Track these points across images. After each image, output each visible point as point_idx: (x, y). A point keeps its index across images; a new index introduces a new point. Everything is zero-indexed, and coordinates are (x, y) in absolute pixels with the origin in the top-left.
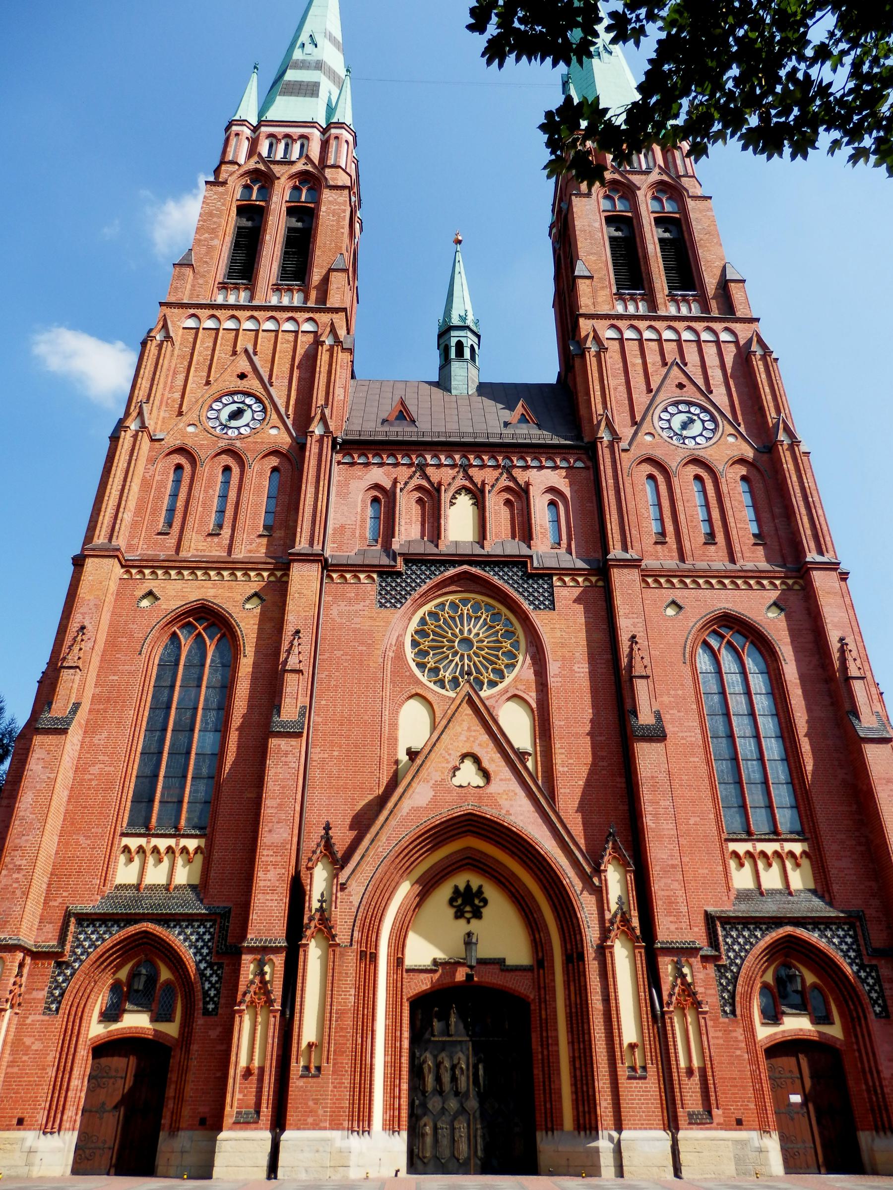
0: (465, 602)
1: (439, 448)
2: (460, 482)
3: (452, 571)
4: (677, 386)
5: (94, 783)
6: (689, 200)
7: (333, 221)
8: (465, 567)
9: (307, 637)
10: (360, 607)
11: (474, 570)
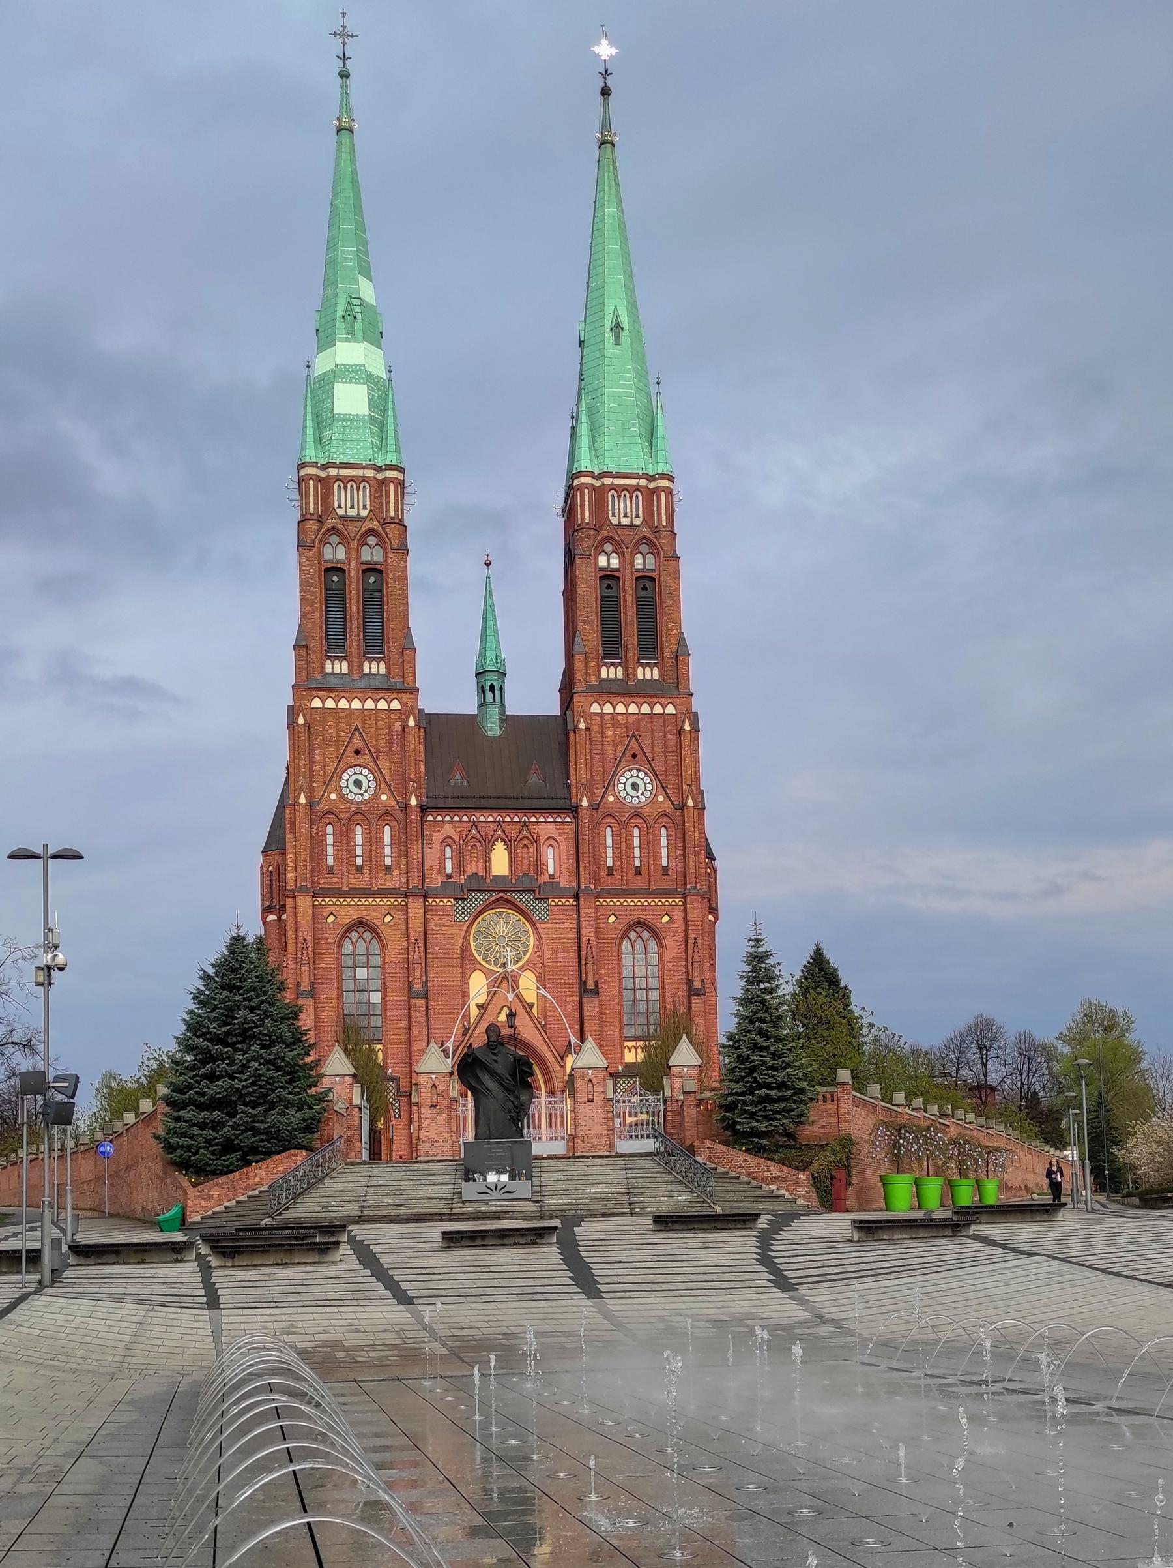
0: (501, 913)
1: (485, 810)
2: (499, 832)
3: (495, 896)
4: (634, 754)
5: (326, 1020)
6: (662, 560)
7: (399, 589)
8: (501, 894)
9: (421, 944)
10: (444, 921)
11: (507, 895)
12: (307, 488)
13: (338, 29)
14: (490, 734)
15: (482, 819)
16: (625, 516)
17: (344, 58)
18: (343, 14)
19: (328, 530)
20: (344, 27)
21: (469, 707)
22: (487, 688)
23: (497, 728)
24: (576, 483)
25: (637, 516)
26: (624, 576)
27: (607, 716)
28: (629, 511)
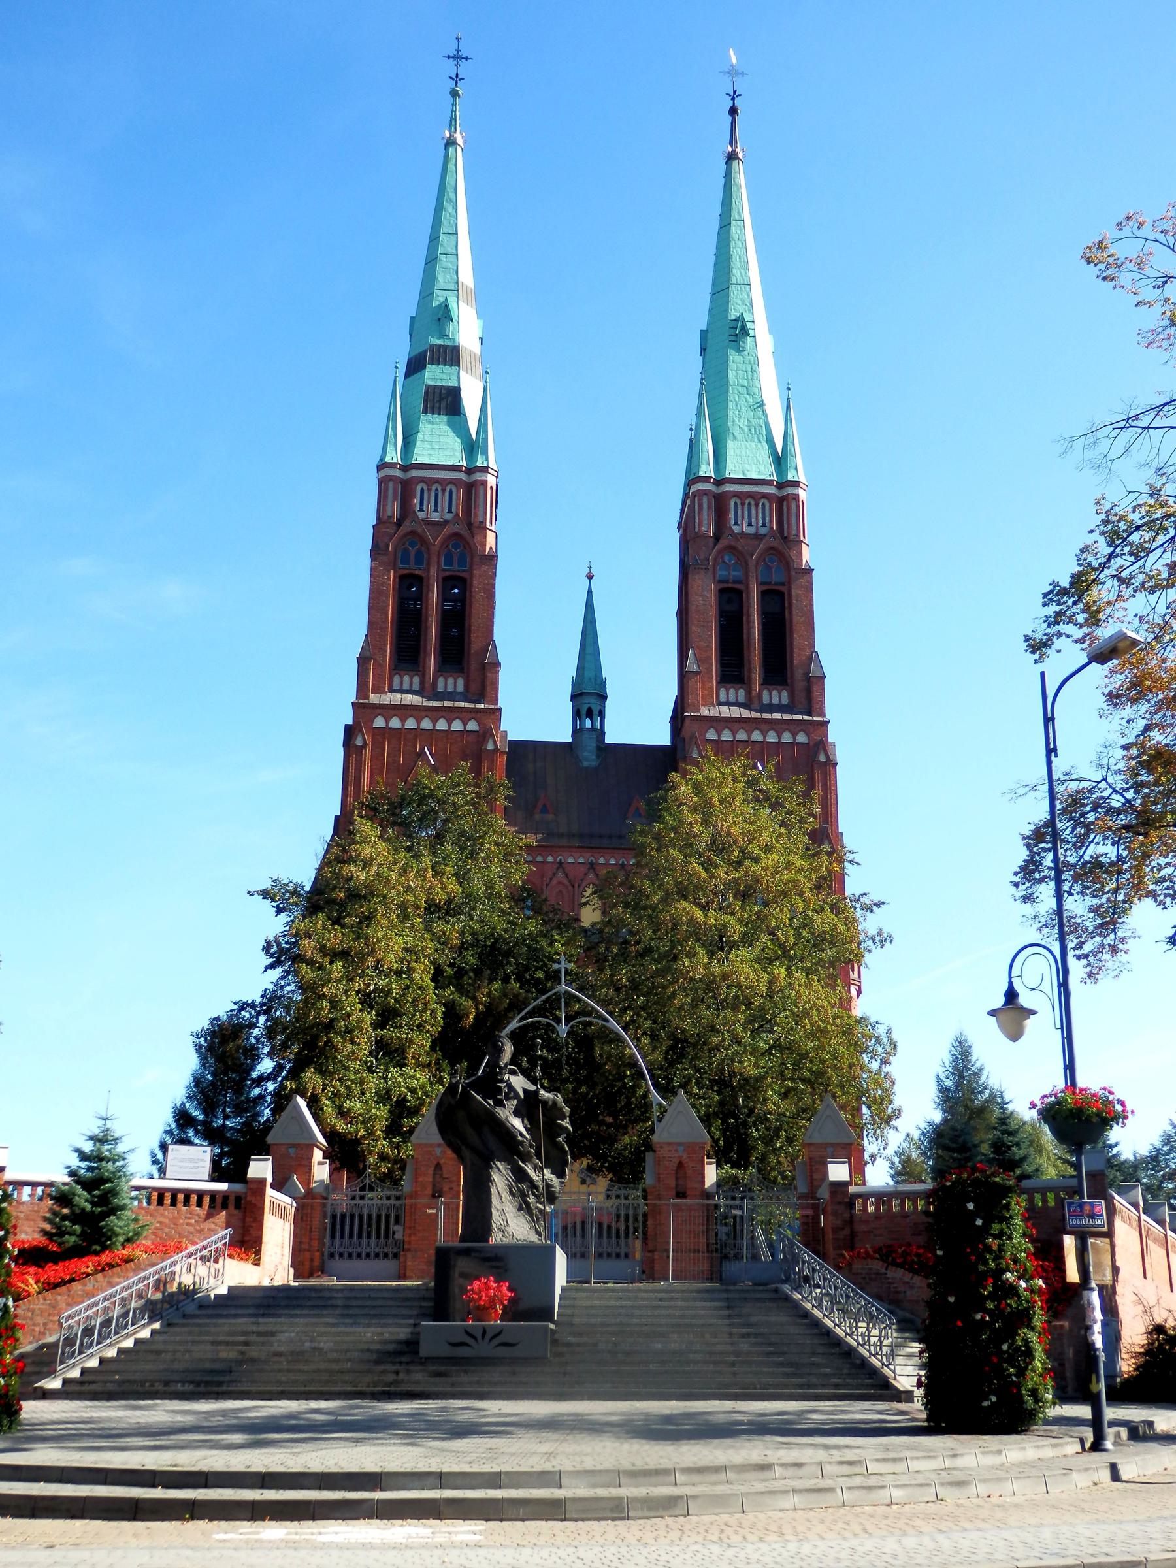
2: (591, 876)
12: (386, 490)
13: (452, 52)
14: (586, 764)
15: (571, 860)
16: (750, 524)
17: (457, 79)
18: (458, 40)
19: (405, 535)
20: (458, 51)
21: (564, 734)
22: (584, 712)
23: (594, 757)
24: (694, 489)
25: (764, 525)
26: (748, 587)
27: (725, 743)
28: (753, 520)
